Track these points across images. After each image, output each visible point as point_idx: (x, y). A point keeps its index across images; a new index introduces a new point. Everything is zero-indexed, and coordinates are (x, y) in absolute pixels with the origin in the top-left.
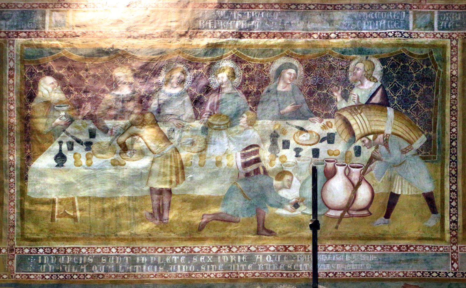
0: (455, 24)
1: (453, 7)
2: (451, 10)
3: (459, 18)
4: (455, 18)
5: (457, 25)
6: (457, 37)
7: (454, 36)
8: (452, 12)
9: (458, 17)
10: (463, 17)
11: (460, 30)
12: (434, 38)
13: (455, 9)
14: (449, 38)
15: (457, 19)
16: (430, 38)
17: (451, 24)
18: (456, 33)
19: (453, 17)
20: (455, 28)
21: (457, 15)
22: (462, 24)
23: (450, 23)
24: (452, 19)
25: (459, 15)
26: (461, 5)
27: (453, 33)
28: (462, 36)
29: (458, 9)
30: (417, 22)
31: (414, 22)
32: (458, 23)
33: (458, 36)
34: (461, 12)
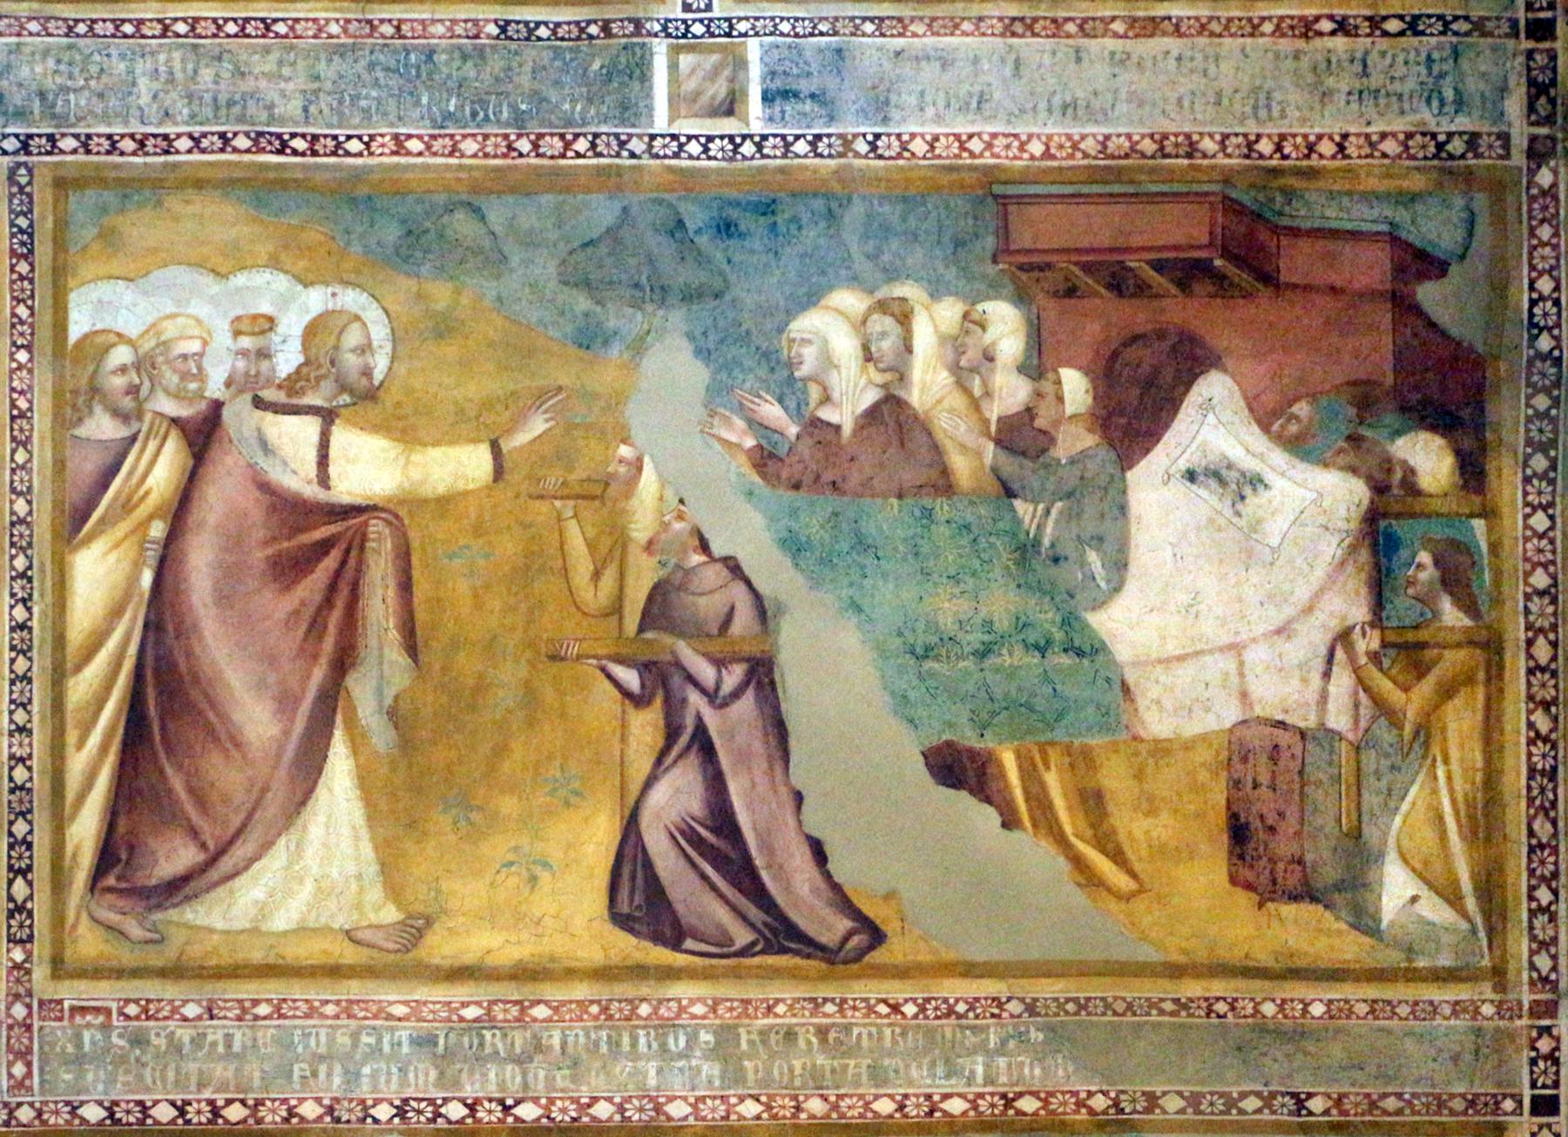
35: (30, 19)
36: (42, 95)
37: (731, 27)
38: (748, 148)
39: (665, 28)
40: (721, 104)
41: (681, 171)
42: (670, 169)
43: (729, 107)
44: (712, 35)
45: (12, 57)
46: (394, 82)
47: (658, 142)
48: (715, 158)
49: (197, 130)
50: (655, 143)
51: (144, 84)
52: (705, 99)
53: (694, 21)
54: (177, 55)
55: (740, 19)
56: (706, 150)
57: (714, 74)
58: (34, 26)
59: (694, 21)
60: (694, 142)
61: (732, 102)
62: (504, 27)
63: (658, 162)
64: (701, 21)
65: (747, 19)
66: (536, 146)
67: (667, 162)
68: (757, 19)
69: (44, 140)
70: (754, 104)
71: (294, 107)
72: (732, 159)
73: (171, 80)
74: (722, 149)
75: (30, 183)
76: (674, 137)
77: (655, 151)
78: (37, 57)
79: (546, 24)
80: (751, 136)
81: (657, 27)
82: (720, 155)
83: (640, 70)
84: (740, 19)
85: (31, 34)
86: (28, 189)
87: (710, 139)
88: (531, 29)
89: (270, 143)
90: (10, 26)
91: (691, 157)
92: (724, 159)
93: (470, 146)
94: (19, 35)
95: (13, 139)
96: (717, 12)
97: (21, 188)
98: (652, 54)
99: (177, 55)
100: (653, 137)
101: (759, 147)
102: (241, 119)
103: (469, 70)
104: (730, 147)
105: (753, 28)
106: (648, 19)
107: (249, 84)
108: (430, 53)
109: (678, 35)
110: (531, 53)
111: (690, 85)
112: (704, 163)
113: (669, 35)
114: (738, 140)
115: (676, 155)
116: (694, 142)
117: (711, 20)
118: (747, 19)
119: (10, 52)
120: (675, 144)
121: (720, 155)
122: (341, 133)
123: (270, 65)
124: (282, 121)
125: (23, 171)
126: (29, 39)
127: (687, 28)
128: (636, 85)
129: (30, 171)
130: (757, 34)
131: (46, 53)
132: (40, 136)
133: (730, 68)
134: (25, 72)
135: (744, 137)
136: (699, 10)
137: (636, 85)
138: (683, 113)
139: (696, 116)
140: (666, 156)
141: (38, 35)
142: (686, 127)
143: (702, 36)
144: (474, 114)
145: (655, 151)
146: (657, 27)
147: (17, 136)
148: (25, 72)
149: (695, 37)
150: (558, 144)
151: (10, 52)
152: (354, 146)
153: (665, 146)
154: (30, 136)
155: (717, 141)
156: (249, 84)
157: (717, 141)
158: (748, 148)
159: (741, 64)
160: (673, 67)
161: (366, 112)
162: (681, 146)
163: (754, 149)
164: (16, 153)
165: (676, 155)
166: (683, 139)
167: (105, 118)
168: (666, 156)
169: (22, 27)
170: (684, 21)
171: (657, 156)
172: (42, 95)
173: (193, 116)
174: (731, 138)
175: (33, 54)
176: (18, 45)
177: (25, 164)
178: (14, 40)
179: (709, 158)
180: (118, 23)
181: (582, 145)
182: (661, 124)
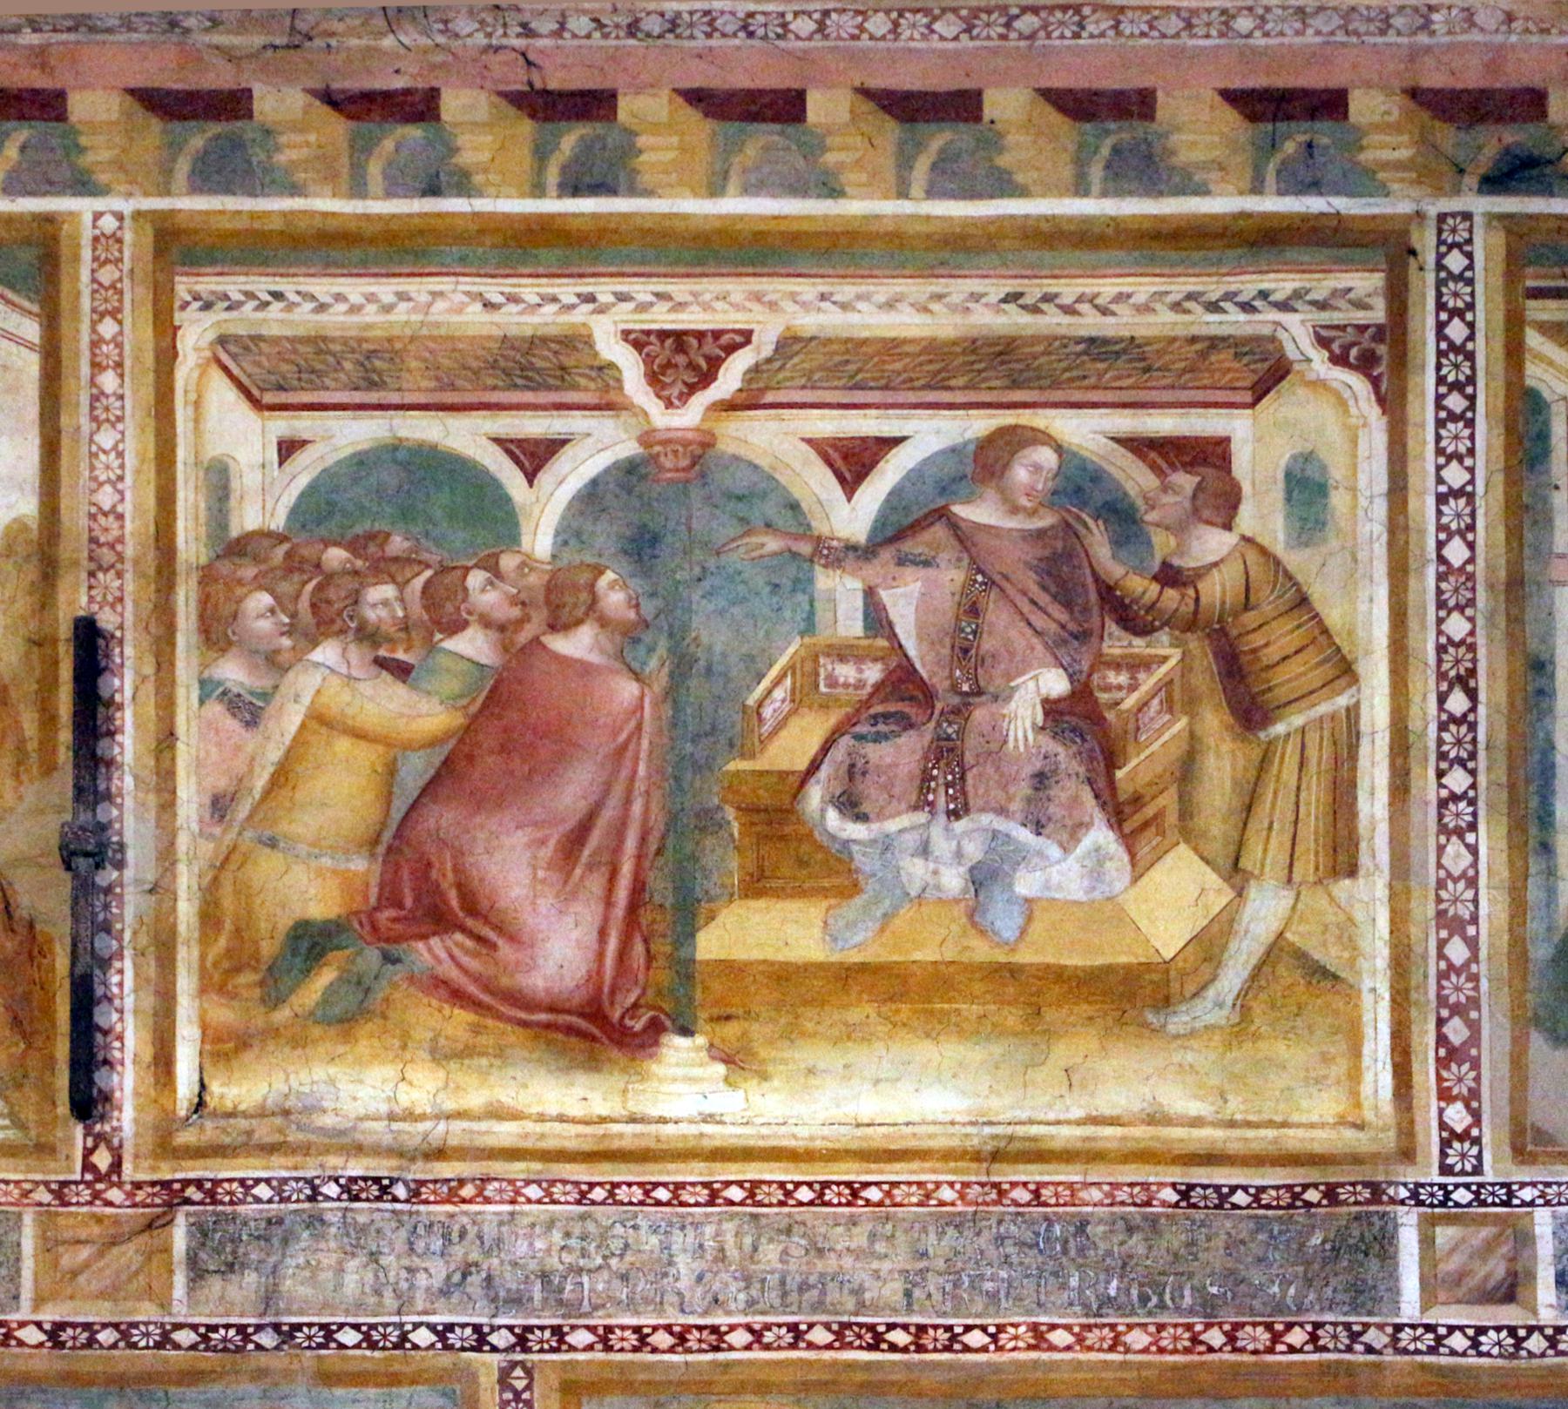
35: (528, 1183)
36: (544, 1276)
37: (1510, 1194)
38: (1536, 1343)
39: (1415, 1195)
40: (1496, 1288)
41: (1440, 1370)
42: (1423, 1367)
43: (1511, 1290)
44: (1483, 1203)
45: (504, 1229)
46: (1032, 1259)
47: (1405, 1335)
48: (1488, 1354)
49: (758, 1320)
50: (1402, 1335)
51: (685, 1266)
52: (1472, 1282)
53: (1457, 1186)
54: (730, 1227)
55: (1523, 1185)
56: (1475, 1344)
57: (1489, 1247)
58: (533, 1192)
59: (1457, 1186)
60: (1458, 1334)
61: (1513, 1286)
62: (1185, 1192)
63: (1407, 1358)
64: (1467, 1186)
65: (1534, 1184)
66: (1231, 1338)
67: (1418, 1358)
68: (1548, 1185)
69: (547, 1334)
70: (1546, 1292)
71: (892, 1291)
72: (1513, 1356)
73: (721, 1256)
74: (1499, 1343)
75: (528, 1387)
76: (1429, 1328)
77: (1402, 1344)
78: (538, 1230)
79: (1245, 1189)
80: (1541, 1329)
81: (1403, 1193)
82: (1495, 1351)
83: (1383, 1245)
84: (1523, 1185)
85: (529, 1201)
86: (526, 1396)
87: (1482, 1330)
88: (1223, 1196)
89: (859, 1337)
90: (501, 1191)
91: (1453, 1353)
92: (1501, 1356)
93: (1138, 1339)
94: (513, 1202)
95: (504, 1332)
96: (1489, 1176)
97: (517, 1395)
98: (1396, 1226)
99: (730, 1227)
100: (1399, 1328)
101: (1553, 1342)
102: (819, 1306)
103: (1136, 1244)
104: (1510, 1341)
105: (1543, 1195)
106: (1390, 1183)
107: (831, 1263)
108: (1082, 1225)
109: (1436, 1205)
110: (1225, 1224)
111: (1451, 1265)
112: (1473, 1360)
113: (1420, 1203)
114: (1522, 1333)
115: (1432, 1350)
116: (1458, 1334)
117: (1481, 1185)
118: (1534, 1184)
119: (501, 1223)
120: (1430, 1336)
121: (1495, 1351)
122: (958, 1322)
123: (860, 1238)
124: (876, 1309)
125: (518, 1372)
126: (527, 1207)
127: (1447, 1194)
128: (1374, 1264)
129: (529, 1373)
130: (1548, 1203)
131: (551, 1224)
132: (542, 1328)
133: (1511, 1244)
134: (522, 1248)
135: (1531, 1330)
136: (1463, 1173)
137: (1374, 1264)
138: (1442, 1296)
139: (1459, 1302)
140: (1417, 1352)
141: (539, 1202)
142: (1444, 1316)
143: (1469, 1205)
144: (1144, 1299)
145: (1402, 1344)
146: (1403, 1193)
147: (511, 1328)
148: (522, 1248)
149: (1457, 1205)
150: (1264, 1336)
151: (501, 1223)
152: (976, 1338)
153: (1415, 1339)
154: (529, 1329)
155: (1492, 1333)
156: (831, 1263)
157: (1492, 1333)
158: (1536, 1343)
159: (1525, 1239)
160: (1427, 1242)
161: (993, 1297)
162: (1439, 1340)
163: (1545, 1344)
164: (510, 1349)
165: (1432, 1350)
166: (1442, 1331)
167: (631, 1305)
168: (1417, 1352)
169: (518, 1193)
170: (1443, 1187)
171: (1405, 1351)
172: (544, 1276)
173: (751, 1303)
174: (1512, 1331)
175: (533, 1225)
176: (512, 1214)
177: (522, 1363)
178: (507, 1208)
179: (1480, 1354)
180: (648, 1188)
181: (1297, 1337)
182: (1410, 1305)
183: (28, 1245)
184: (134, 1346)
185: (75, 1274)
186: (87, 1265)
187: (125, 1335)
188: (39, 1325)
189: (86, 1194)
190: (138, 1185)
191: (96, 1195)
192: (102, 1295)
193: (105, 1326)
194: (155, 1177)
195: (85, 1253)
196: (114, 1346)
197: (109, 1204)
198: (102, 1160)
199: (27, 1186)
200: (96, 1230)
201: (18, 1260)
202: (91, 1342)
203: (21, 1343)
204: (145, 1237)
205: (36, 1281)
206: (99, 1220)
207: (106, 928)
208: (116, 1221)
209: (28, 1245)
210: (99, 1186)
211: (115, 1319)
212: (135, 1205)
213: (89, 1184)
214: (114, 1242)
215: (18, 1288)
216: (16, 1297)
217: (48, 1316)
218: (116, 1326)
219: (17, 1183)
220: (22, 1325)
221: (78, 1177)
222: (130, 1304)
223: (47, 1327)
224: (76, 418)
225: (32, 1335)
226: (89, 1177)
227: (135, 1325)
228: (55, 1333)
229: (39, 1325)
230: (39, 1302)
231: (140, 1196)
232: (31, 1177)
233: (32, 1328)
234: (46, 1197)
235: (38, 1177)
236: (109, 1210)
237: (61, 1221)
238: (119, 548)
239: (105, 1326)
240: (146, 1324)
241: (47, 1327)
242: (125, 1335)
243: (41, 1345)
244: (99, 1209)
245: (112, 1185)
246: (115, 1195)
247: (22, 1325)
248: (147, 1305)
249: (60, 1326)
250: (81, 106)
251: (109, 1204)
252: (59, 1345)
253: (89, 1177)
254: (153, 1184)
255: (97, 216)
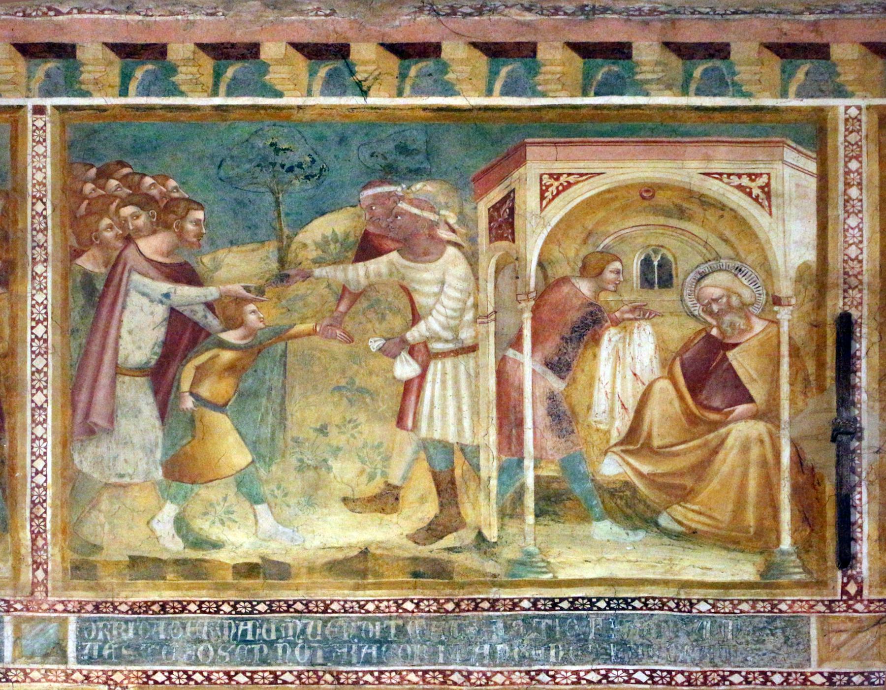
0: (120, 648)
1: (115, 608)
2: (111, 615)
3: (131, 634)
4: (119, 634)
5: (124, 652)
6: (126, 682)
7: (118, 677)
8: (113, 618)
9: (126, 631)
10: (141, 632)
11: (131, 663)
12: (66, 681)
13: (121, 612)
14: (105, 683)
15: (125, 637)
16: (57, 681)
17: (110, 648)
18: (121, 671)
19: (115, 632)
20: (119, 658)
21: (124, 627)
22: (137, 649)
23: (107, 646)
24: (112, 636)
25: (131, 626)
26: (134, 603)
27: (114, 672)
28: (137, 678)
29: (127, 613)
30: (24, 642)
31: (15, 642)
32: (128, 647)
33: (127, 677)
34: (135, 620)
183: (814, 632)
184: (873, 684)
185: (838, 648)
186: (844, 643)
187: (868, 678)
188: (822, 674)
189: (844, 607)
190: (871, 602)
191: (849, 607)
192: (854, 658)
193: (856, 674)
194: (880, 597)
195: (844, 636)
196: (862, 684)
197: (856, 611)
198: (852, 589)
199: (812, 603)
200: (850, 624)
201: (809, 641)
202: (849, 682)
203: (813, 683)
204: (876, 629)
205: (819, 651)
206: (851, 619)
207: (853, 471)
208: (860, 620)
209: (814, 632)
210: (851, 602)
211: (861, 670)
212: (870, 612)
213: (845, 602)
214: (860, 630)
215: (809, 654)
216: (809, 660)
217: (827, 669)
218: (862, 674)
219: (807, 601)
220: (813, 674)
221: (839, 598)
222: (869, 663)
223: (826, 674)
224: (837, 211)
225: (818, 679)
226: (845, 598)
227: (873, 673)
228: (830, 677)
229: (822, 674)
230: (821, 662)
231: (873, 607)
232: (815, 598)
233: (818, 675)
234: (823, 609)
235: (819, 598)
236: (856, 615)
237: (831, 620)
238: (860, 277)
239: (856, 674)
240: (879, 672)
241: (826, 674)
242: (868, 678)
243: (823, 684)
244: (851, 614)
245: (858, 601)
246: (859, 607)
247: (813, 674)
248: (878, 663)
249: (832, 674)
250: (837, 52)
251: (856, 611)
252: (832, 684)
253: (845, 598)
254: (880, 601)
255: (847, 108)
